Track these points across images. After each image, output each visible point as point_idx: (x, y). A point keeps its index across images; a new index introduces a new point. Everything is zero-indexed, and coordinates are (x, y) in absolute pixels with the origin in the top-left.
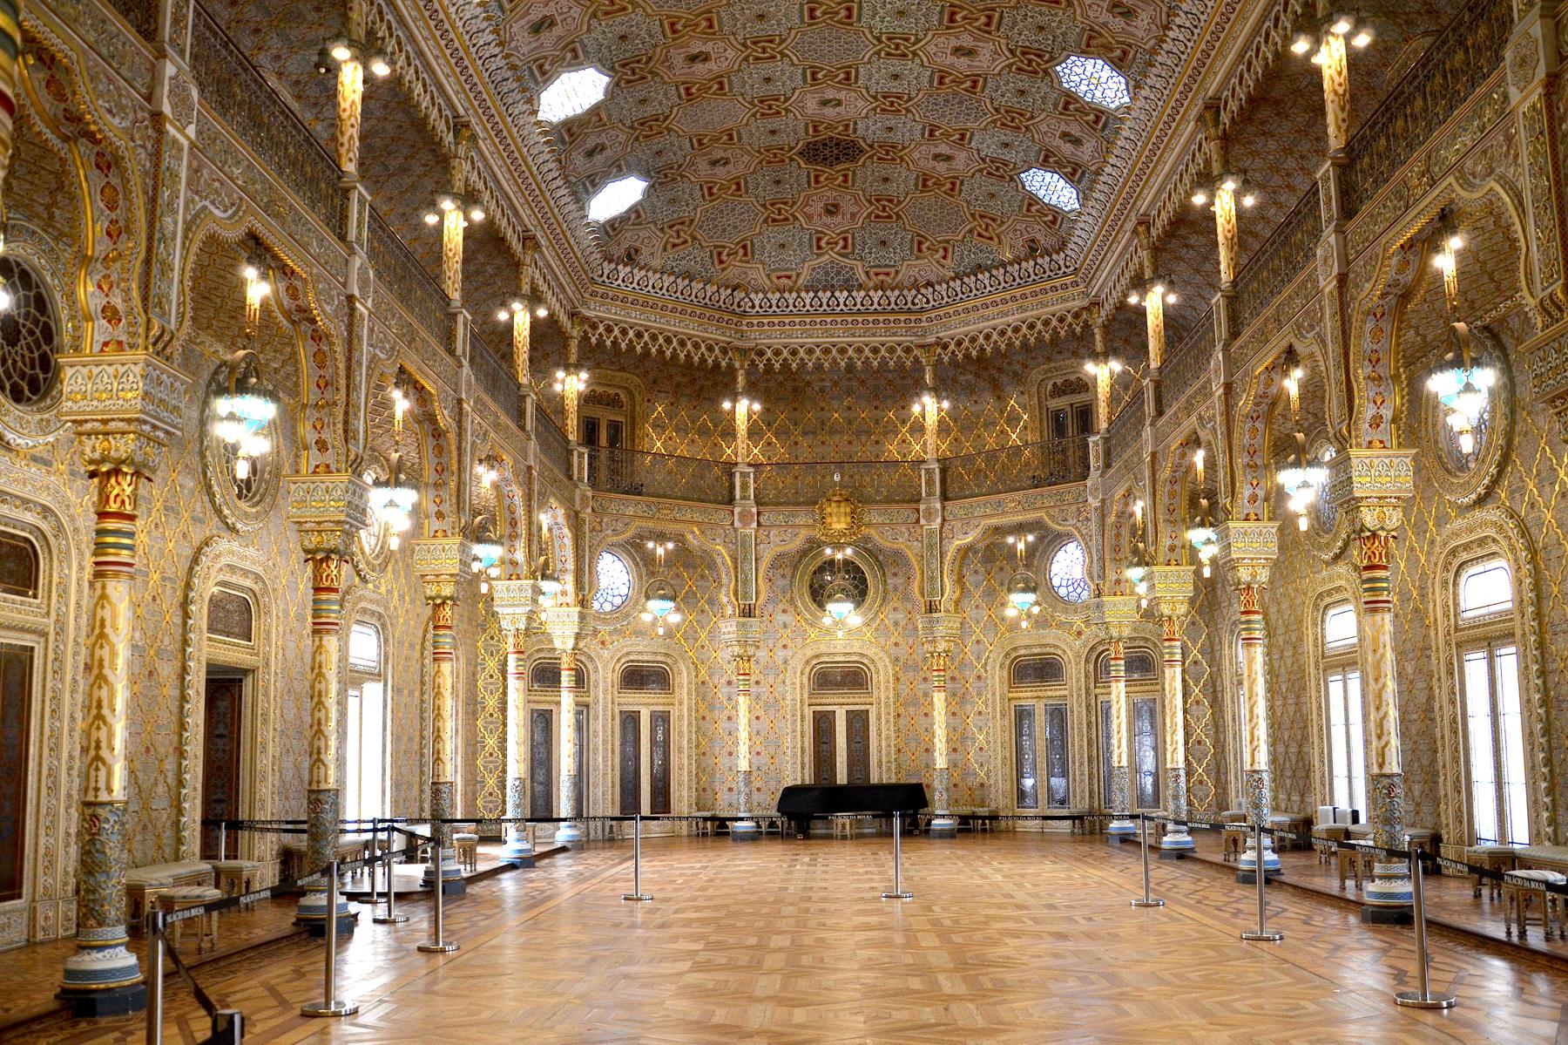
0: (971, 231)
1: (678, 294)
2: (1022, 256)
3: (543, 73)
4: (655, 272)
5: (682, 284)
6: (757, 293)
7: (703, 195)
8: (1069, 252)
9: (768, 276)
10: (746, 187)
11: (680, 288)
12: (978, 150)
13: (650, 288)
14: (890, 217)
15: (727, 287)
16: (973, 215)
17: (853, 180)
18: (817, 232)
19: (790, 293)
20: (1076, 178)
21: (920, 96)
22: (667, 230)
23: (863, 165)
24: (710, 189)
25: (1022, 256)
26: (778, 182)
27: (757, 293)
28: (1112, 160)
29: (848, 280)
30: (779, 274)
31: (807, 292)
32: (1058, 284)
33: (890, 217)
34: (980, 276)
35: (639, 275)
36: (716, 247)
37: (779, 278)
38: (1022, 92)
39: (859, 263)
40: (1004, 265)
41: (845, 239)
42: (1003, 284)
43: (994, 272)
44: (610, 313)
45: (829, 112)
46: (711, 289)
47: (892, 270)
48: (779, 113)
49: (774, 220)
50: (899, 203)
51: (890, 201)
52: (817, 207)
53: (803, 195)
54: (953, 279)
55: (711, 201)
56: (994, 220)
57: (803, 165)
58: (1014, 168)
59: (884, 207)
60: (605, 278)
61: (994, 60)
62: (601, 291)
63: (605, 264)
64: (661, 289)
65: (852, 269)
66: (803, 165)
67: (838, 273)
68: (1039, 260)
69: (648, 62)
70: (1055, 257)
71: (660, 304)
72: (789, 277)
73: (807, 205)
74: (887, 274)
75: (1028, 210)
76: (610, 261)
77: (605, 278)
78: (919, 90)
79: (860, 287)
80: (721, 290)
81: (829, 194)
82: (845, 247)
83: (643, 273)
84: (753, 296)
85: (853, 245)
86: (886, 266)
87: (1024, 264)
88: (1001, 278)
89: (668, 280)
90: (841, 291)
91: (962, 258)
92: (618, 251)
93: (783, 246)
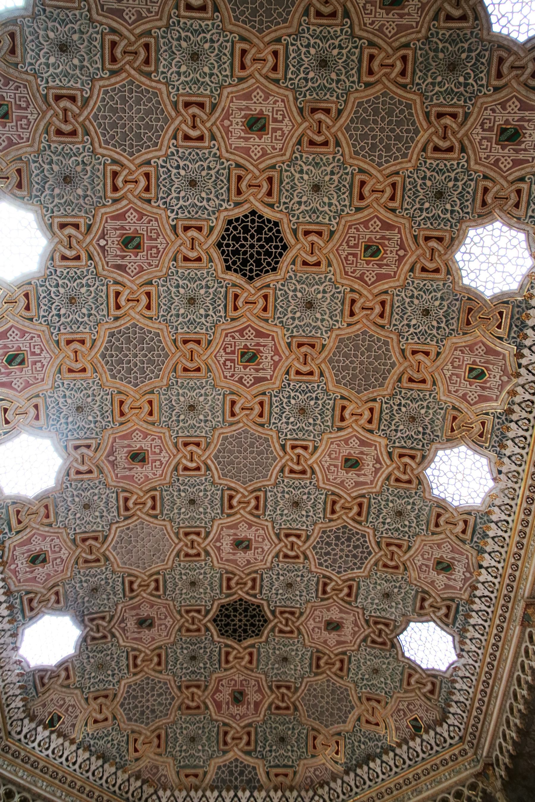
0: (359, 719)
1: (90, 774)
2: (408, 737)
3: (32, 609)
4: (72, 742)
5: (96, 763)
6: (165, 790)
7: (128, 665)
8: (450, 722)
9: (178, 773)
10: (167, 662)
11: (93, 768)
12: (363, 609)
13: (63, 759)
14: (287, 708)
15: (137, 778)
16: (360, 698)
17: (258, 661)
18: (225, 724)
19: (196, 791)
20: (450, 621)
21: (316, 531)
22: (91, 701)
23: (267, 641)
24: (135, 658)
25: (408, 737)
26: (193, 658)
27: (165, 790)
28: (484, 576)
29: (249, 781)
30: (188, 771)
31: (212, 791)
32: (447, 757)
33: (287, 708)
34: (372, 765)
35: (56, 742)
36: (133, 732)
37: (187, 776)
38: (399, 514)
39: (260, 762)
40: (393, 750)
41: (249, 734)
42: (394, 769)
43: (385, 758)
44: (17, 775)
45: (241, 556)
46: (122, 777)
47: (290, 771)
48: (198, 555)
49: (188, 708)
50: (297, 689)
51: (288, 688)
52: (225, 695)
53: (214, 677)
54: (347, 773)
55: (135, 674)
56: (379, 702)
57: (216, 638)
58: (395, 627)
59: (283, 695)
60: (22, 736)
61: (377, 471)
62: (14, 748)
63: (26, 721)
64: (74, 764)
65: (254, 768)
66: (216, 638)
67: (241, 773)
68: (425, 737)
69: (96, 450)
70: (438, 729)
71: (69, 779)
72: (196, 776)
73: (217, 690)
74: (286, 775)
75: (409, 684)
76: (31, 720)
77: (22, 736)
78: (315, 524)
79: (260, 788)
80: (132, 780)
81: (236, 678)
82: (248, 743)
83: (61, 740)
84: (161, 793)
85: (256, 742)
86: (285, 766)
87: (411, 744)
88: (391, 763)
89: (83, 755)
90: (244, 791)
91: (353, 751)
92: (44, 714)
93: (193, 740)
